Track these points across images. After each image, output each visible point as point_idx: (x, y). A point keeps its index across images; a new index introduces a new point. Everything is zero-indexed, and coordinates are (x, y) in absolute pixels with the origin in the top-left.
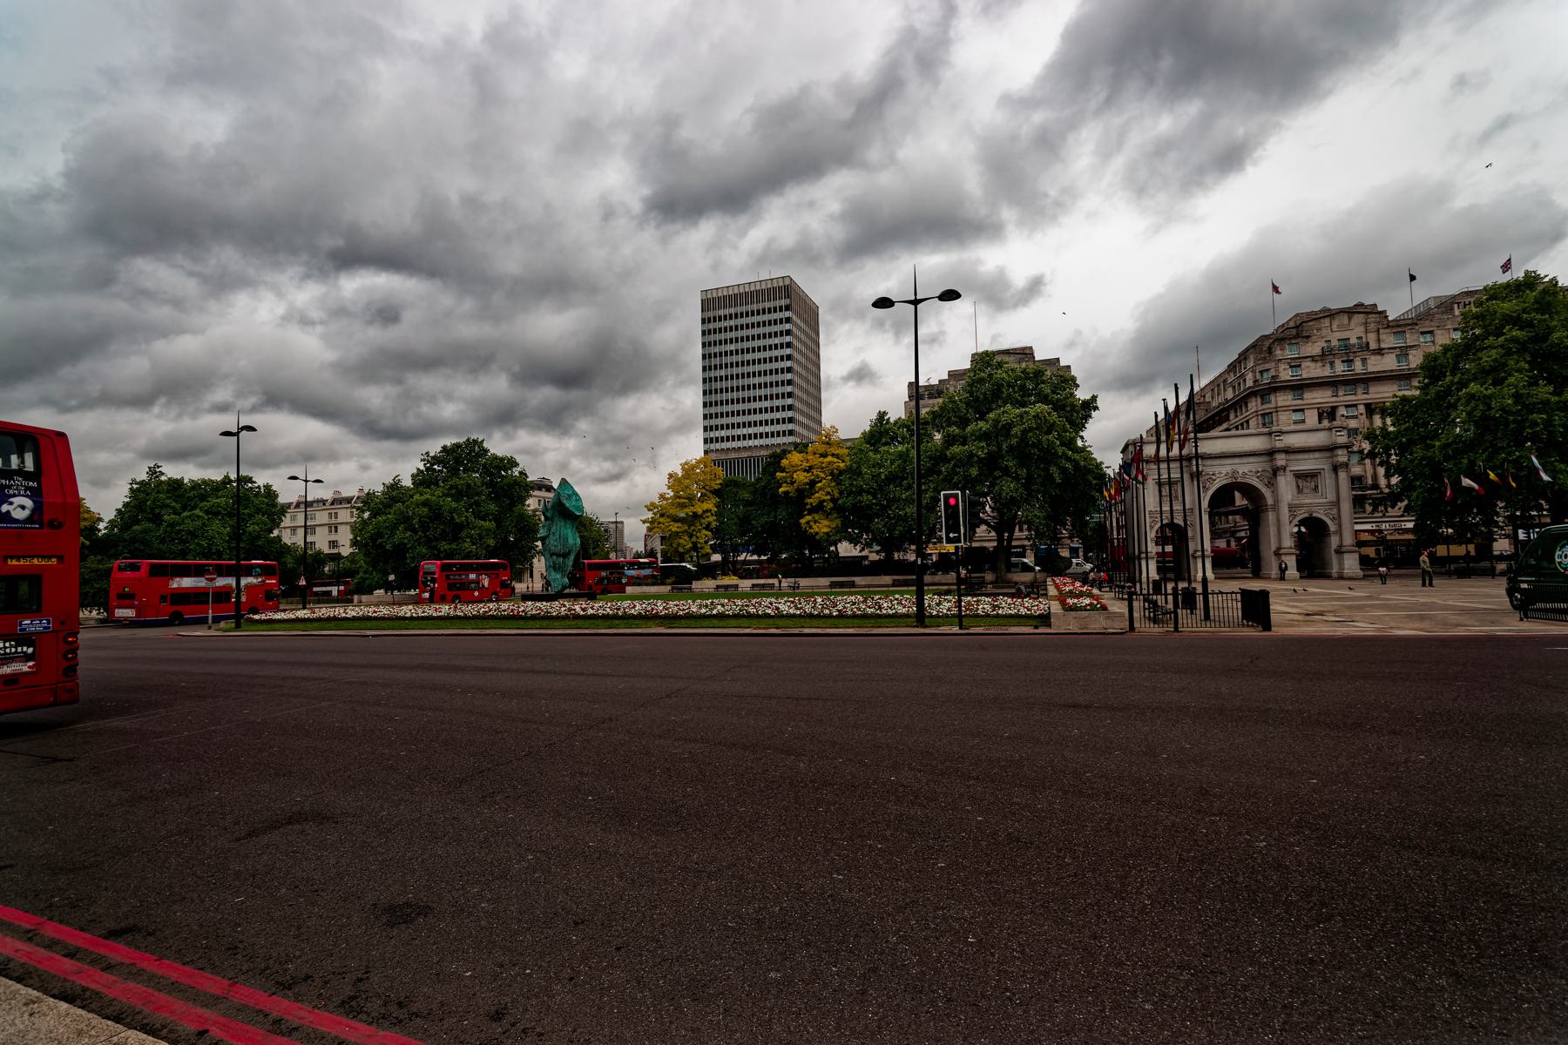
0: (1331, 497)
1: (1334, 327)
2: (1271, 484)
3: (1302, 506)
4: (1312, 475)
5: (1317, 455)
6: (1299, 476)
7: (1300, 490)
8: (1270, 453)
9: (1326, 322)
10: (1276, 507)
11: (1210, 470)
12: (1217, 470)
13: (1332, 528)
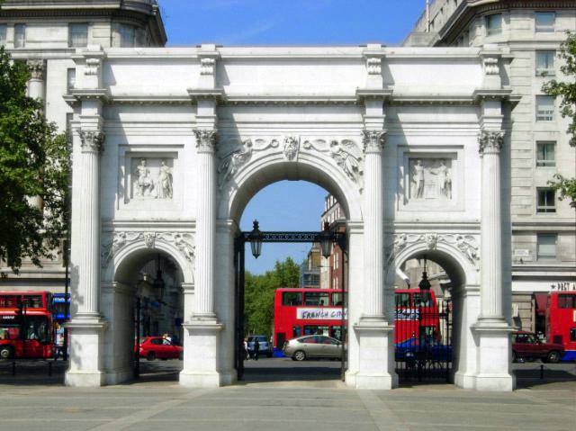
4: (440, 159)
13: (471, 277)
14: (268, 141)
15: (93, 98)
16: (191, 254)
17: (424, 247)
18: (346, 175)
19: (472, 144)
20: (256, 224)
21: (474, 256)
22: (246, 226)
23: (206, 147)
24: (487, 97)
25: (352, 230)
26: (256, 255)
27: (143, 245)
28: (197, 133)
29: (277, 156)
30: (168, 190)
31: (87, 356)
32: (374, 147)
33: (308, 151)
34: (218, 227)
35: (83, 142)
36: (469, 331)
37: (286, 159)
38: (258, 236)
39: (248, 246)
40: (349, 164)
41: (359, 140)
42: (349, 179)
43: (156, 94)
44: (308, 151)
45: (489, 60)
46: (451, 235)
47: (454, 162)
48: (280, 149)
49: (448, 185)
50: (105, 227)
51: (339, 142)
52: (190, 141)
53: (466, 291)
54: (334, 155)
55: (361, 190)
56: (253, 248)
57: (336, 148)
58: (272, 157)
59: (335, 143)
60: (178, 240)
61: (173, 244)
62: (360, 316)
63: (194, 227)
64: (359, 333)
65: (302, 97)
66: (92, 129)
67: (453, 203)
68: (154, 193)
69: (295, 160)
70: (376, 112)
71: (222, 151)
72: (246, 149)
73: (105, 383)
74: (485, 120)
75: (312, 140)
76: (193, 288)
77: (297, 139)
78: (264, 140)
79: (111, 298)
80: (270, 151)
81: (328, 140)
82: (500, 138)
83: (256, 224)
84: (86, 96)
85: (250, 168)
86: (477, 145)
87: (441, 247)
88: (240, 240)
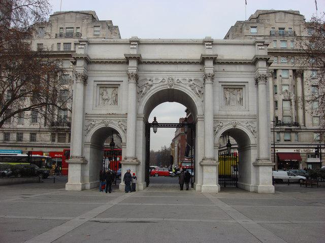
0: (253, 111)
1: (277, 19)
2: (201, 93)
3: (227, 117)
4: (239, 87)
5: (242, 68)
6: (228, 87)
7: (228, 103)
8: (202, 61)
9: (273, 15)
10: (203, 118)
11: (148, 76)
12: (154, 76)
13: (252, 141)
14: (161, 79)
15: (82, 58)
16: (125, 130)
17: (231, 127)
18: (196, 95)
19: (251, 81)
20: (155, 118)
21: (254, 131)
22: (151, 120)
23: (133, 81)
24: (260, 58)
25: (199, 119)
26: (155, 132)
27: (103, 126)
28: (128, 75)
29: (165, 86)
30: (116, 102)
31: (75, 176)
32: (208, 81)
33: (179, 84)
34: (138, 117)
35: (77, 78)
36: (252, 165)
37: (169, 88)
38: (156, 125)
39: (152, 129)
40: (197, 90)
41: (201, 79)
42: (197, 96)
43: (110, 58)
44: (179, 84)
45: (259, 44)
46: (242, 122)
47: (244, 89)
48: (166, 83)
49: (241, 99)
50: (86, 116)
51: (193, 79)
52: (125, 79)
53: (250, 147)
54: (190, 86)
55: (202, 101)
56: (154, 129)
57: (191, 83)
58: (163, 87)
59: (191, 80)
60: (120, 123)
61: (117, 125)
62: (202, 158)
63: (127, 117)
64: (202, 166)
65: (176, 60)
66: (80, 72)
67: (243, 107)
68: (110, 102)
69: (173, 88)
70: (209, 64)
71: (141, 84)
72: (150, 83)
73: (83, 189)
74: (259, 69)
75: (180, 79)
76: (126, 145)
77: (174, 78)
78: (159, 79)
79: (88, 150)
80: (162, 84)
81: (187, 79)
82: (266, 77)
83: (155, 118)
84: (78, 57)
85: (153, 91)
86: (254, 82)
87: (238, 127)
88: (148, 126)
